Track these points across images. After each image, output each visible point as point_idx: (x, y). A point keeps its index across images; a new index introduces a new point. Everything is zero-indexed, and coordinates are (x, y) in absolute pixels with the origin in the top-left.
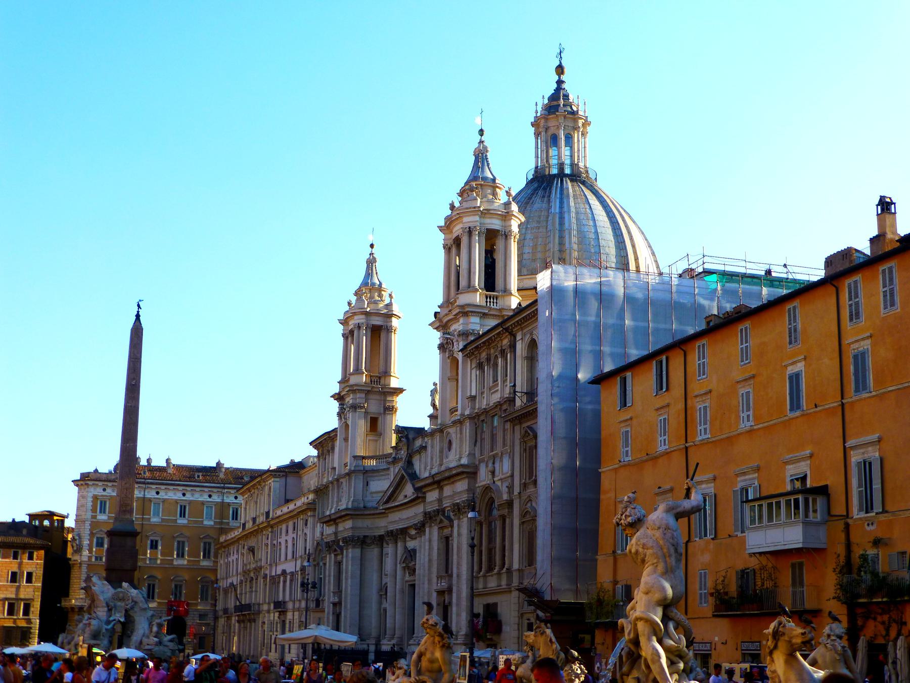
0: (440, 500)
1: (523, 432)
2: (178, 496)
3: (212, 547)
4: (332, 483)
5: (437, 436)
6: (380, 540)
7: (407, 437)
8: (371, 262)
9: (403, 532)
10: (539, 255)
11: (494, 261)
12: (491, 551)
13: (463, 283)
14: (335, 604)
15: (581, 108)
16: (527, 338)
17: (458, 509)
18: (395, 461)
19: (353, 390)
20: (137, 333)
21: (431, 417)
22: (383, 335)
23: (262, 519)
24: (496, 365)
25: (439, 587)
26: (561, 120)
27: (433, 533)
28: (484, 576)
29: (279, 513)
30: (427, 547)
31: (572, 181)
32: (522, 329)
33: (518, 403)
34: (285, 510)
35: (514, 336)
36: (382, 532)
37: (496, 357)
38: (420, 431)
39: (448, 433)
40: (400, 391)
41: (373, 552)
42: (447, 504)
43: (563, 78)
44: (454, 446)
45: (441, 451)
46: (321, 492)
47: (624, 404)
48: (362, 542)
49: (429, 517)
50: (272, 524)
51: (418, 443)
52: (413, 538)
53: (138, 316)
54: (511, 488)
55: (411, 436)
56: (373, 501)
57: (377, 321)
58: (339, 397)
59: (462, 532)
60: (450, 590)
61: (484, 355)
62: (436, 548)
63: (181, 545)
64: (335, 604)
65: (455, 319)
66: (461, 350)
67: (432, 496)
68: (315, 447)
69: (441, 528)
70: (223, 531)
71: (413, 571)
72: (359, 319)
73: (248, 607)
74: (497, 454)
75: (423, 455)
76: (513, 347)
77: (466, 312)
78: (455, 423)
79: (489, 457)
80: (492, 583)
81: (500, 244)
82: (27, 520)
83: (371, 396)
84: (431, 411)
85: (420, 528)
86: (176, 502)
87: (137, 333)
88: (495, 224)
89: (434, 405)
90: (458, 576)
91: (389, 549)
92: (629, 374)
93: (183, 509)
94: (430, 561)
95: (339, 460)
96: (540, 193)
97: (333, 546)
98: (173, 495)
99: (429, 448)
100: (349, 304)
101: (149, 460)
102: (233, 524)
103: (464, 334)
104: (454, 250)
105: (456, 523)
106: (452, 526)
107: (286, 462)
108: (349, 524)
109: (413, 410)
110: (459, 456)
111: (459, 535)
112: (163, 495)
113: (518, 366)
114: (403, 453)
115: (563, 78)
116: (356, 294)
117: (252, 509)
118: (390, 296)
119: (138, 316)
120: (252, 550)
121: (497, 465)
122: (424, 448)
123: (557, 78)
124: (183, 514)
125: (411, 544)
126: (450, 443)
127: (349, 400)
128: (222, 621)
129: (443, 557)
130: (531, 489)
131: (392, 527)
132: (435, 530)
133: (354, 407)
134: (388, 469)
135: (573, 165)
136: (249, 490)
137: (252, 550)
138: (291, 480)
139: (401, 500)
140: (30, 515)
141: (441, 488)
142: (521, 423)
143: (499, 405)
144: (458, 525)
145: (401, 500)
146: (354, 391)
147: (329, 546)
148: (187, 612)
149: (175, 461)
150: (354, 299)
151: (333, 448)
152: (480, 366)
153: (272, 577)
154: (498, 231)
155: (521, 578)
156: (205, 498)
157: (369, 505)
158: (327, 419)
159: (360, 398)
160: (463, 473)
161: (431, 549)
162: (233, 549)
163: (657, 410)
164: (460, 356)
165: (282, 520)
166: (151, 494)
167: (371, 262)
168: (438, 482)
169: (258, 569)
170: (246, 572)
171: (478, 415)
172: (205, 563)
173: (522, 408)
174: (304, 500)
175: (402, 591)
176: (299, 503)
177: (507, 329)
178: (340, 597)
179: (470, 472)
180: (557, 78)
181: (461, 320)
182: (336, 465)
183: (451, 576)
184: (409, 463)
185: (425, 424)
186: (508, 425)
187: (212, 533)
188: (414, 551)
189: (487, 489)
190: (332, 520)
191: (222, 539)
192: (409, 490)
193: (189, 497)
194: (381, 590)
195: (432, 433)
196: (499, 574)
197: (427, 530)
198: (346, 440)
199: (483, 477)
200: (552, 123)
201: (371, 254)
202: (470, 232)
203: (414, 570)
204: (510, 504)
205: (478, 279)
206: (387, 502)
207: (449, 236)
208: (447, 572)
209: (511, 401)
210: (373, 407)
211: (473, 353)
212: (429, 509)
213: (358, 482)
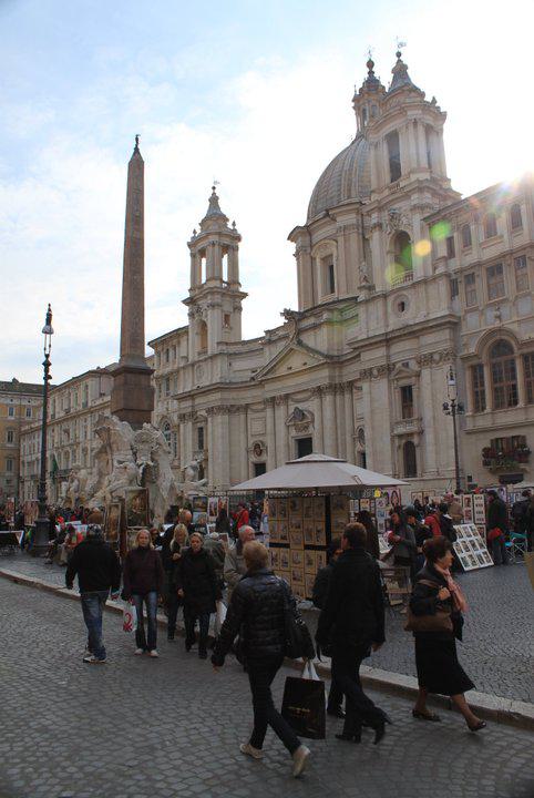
0: (388, 357)
6: (247, 407)
8: (214, 200)
19: (212, 292)
36: (249, 401)
57: (226, 241)
72: (213, 238)
108: (218, 395)
118: (234, 224)
120: (67, 432)
127: (203, 303)
133: (212, 306)
137: (67, 432)
141: (388, 347)
145: (282, 370)
146: (212, 293)
157: (233, 381)
159: (217, 298)
167: (214, 200)
168: (388, 340)
179: (453, 324)
190: (181, 398)
201: (214, 194)
210: (228, 308)
213: (220, 364)
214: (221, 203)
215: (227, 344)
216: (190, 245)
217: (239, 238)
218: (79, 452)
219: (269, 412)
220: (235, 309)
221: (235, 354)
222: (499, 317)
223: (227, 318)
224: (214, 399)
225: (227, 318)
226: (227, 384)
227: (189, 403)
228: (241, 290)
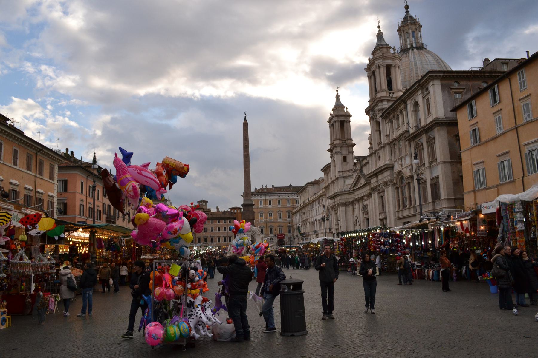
0: (377, 182)
1: (415, 144)
2: (277, 197)
3: (291, 215)
4: (331, 183)
5: (373, 156)
6: (352, 203)
7: (359, 160)
9: (362, 198)
10: (408, 79)
11: (390, 78)
12: (403, 199)
13: (378, 89)
14: (336, 229)
15: (417, 20)
16: (413, 102)
17: (386, 184)
18: (355, 171)
20: (246, 125)
21: (369, 148)
22: (345, 124)
23: (307, 201)
24: (398, 118)
25: (381, 217)
26: (410, 25)
27: (375, 196)
28: (402, 210)
29: (312, 198)
30: (373, 203)
31: (417, 49)
32: (410, 98)
33: (411, 131)
34: (314, 197)
35: (405, 103)
36: (353, 200)
37: (398, 115)
38: (364, 158)
39: (378, 153)
40: (355, 145)
41: (350, 208)
42: (380, 182)
43: (409, 10)
44: (381, 158)
45: (376, 161)
46: (327, 188)
47: (472, 116)
48: (345, 204)
49: (373, 190)
50: (310, 203)
51: (365, 161)
52: (366, 200)
53: (245, 118)
54: (411, 170)
55: (361, 160)
56: (347, 188)
57: (342, 119)
58: (330, 150)
59: (390, 193)
60: (386, 219)
61: (392, 116)
62: (377, 203)
63: (280, 214)
64: (336, 229)
65: (377, 105)
66: (381, 116)
67: (373, 181)
68: (323, 172)
69: (379, 193)
70: (294, 208)
71: (367, 213)
72: (335, 119)
73: (305, 233)
74: (402, 157)
75: (368, 165)
76: (406, 108)
77: (381, 100)
78: (381, 148)
79: (399, 159)
80: (406, 213)
81: (393, 70)
82: (229, 210)
83: (343, 148)
84: (369, 146)
85: (369, 195)
86: (277, 199)
87: (246, 125)
88: (389, 62)
89: (370, 143)
90: (389, 212)
91: (356, 206)
92: (473, 102)
93: (279, 202)
94: (375, 207)
95: (332, 174)
96: (405, 55)
97: (334, 208)
98: (275, 197)
99: (370, 162)
100: (331, 114)
101: (266, 186)
102: (297, 205)
103: (382, 110)
104: (373, 77)
105: (386, 190)
106: (384, 191)
107: (312, 180)
108: (339, 198)
109: (361, 149)
110: (385, 159)
111: (388, 194)
112: (272, 197)
113: (410, 115)
114: (358, 167)
115: (409, 10)
116: (333, 110)
117: (303, 199)
118: (347, 109)
119: (245, 118)
120: (304, 213)
121: (403, 162)
122: (368, 163)
123: (405, 10)
124: (279, 204)
125: (365, 203)
126: (379, 157)
127: (334, 151)
128: (296, 240)
129: (381, 205)
130: (422, 168)
131: (356, 197)
132: (376, 194)
133: (337, 153)
134: (353, 175)
135: (417, 42)
136: (301, 192)
137: (304, 213)
138: (316, 186)
139: (359, 185)
140: (230, 209)
141: (377, 177)
142: (414, 140)
143: (401, 135)
144: (387, 191)
146: (336, 147)
147: (332, 207)
148: (284, 237)
149: (275, 186)
150: (332, 112)
151: (330, 171)
152: (391, 121)
153: (312, 222)
154: (391, 65)
155: (421, 209)
156: (287, 197)
157: (346, 190)
158: (326, 159)
159: (339, 149)
160: (387, 168)
161: (375, 202)
162: (298, 214)
163: (493, 114)
164: (380, 120)
165: (314, 201)
166: (268, 198)
168: (376, 174)
169: (307, 220)
170: (303, 221)
171: (392, 142)
172: (289, 220)
173: (414, 133)
174: (321, 192)
175: (363, 222)
176: (319, 194)
177: (402, 100)
178: (338, 226)
179: (390, 168)
180: (405, 10)
181: (379, 104)
182: (332, 176)
183: (386, 212)
184: (361, 171)
185: (366, 153)
186: (407, 143)
187: (290, 209)
188: (367, 205)
189: (400, 172)
190: (332, 198)
191: (294, 211)
192: (363, 181)
193: (281, 197)
194: (354, 222)
195: (370, 155)
196: (409, 208)
197: (373, 195)
198: (335, 166)
199: (397, 168)
200: (406, 28)
201: (337, 94)
202: (379, 67)
203: (368, 213)
204: (412, 177)
205: (385, 86)
206: (354, 187)
207: (369, 72)
208: (383, 210)
209: (408, 131)
210: (345, 152)
211: (386, 116)
212: (372, 186)
213: (341, 181)
214: (341, 98)
215: (342, 172)
216: (328, 122)
217: (350, 116)
218: (308, 223)
219: (357, 205)
220: (349, 152)
221: (346, 177)
222: (402, 165)
223: (345, 159)
224: (338, 199)
225: (345, 159)
226: (342, 192)
227: (333, 201)
228: (354, 142)
